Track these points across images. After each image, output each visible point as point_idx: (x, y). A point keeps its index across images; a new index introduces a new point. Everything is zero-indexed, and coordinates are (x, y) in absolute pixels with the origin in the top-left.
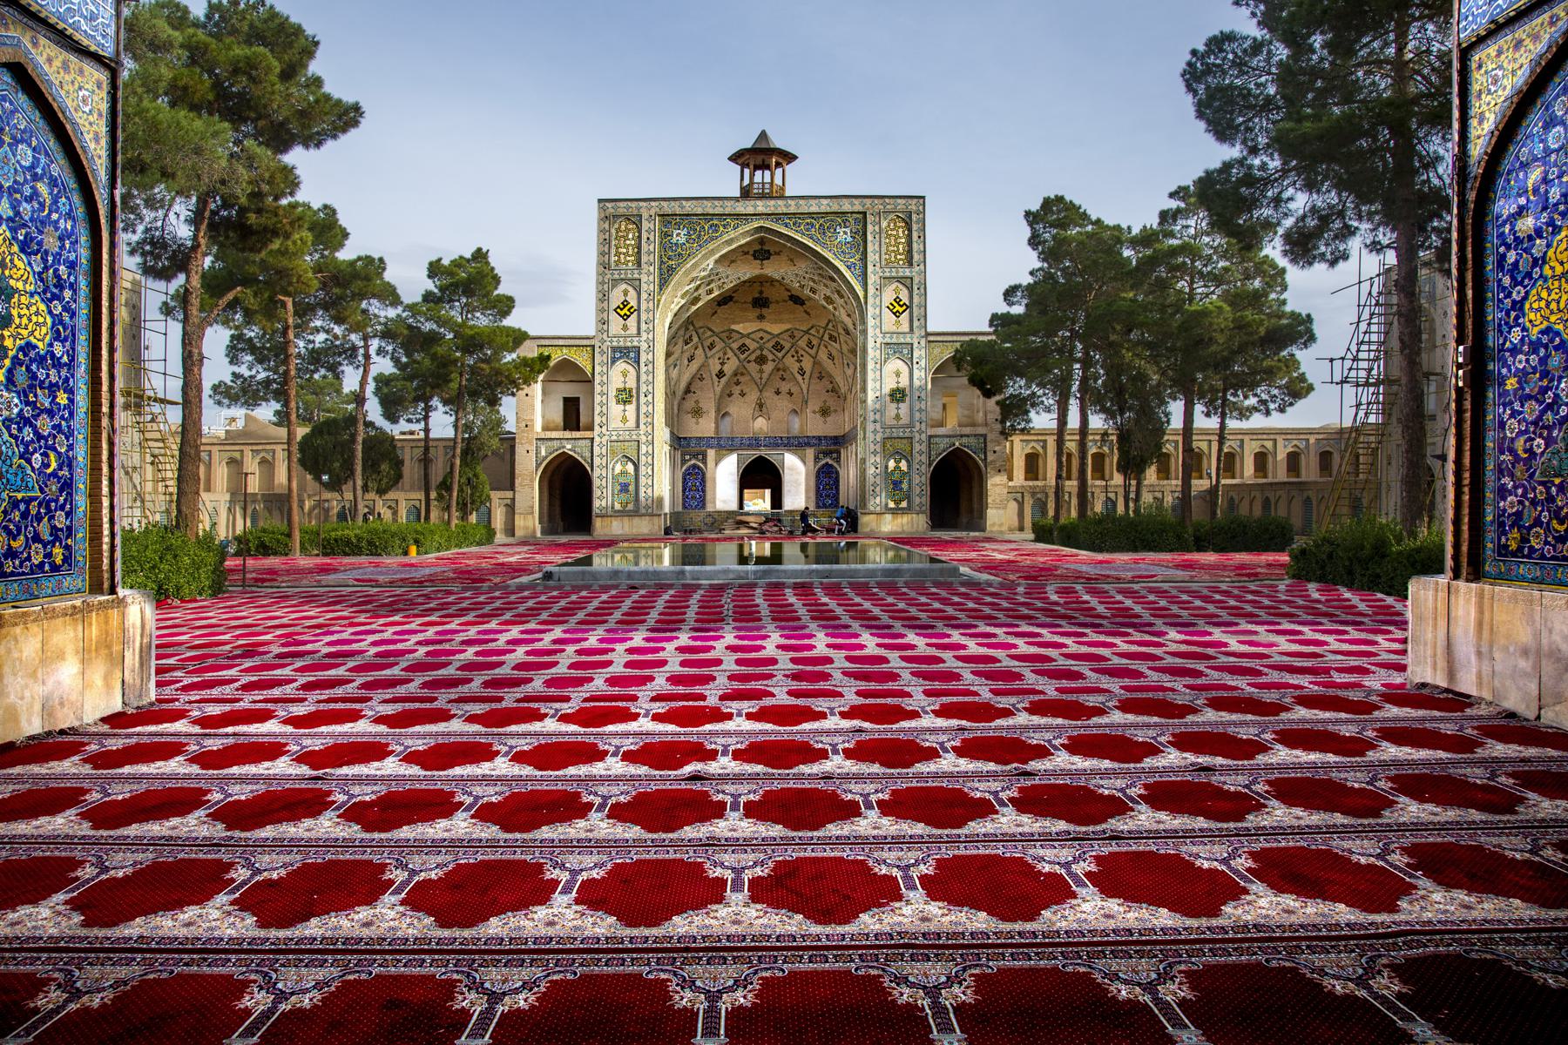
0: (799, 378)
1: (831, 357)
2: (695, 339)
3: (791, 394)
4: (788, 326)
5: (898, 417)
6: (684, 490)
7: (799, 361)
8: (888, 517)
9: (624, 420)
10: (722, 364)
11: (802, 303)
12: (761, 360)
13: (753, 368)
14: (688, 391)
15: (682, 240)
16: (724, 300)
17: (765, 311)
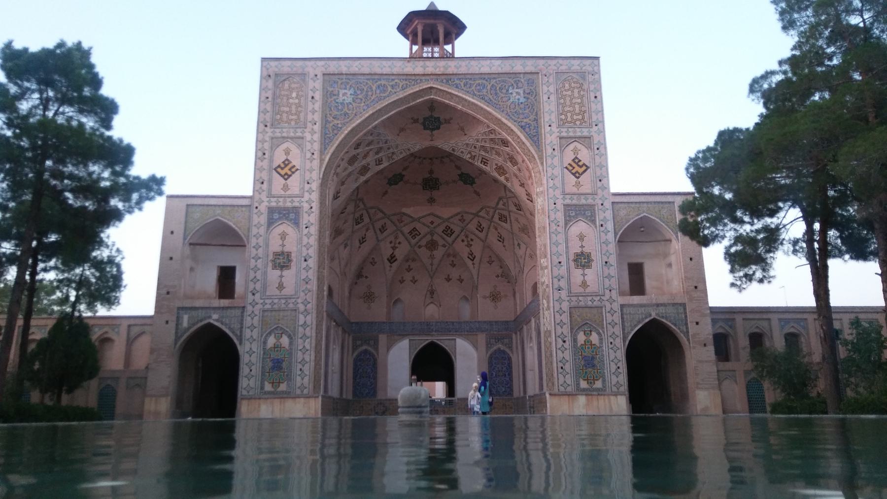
0: (469, 263)
1: (501, 239)
2: (366, 220)
3: (461, 281)
4: (458, 210)
6: (355, 378)
7: (469, 246)
8: (582, 399)
10: (394, 248)
11: (472, 183)
12: (432, 245)
13: (424, 253)
14: (359, 275)
15: (349, 99)
16: (395, 179)
17: (435, 193)
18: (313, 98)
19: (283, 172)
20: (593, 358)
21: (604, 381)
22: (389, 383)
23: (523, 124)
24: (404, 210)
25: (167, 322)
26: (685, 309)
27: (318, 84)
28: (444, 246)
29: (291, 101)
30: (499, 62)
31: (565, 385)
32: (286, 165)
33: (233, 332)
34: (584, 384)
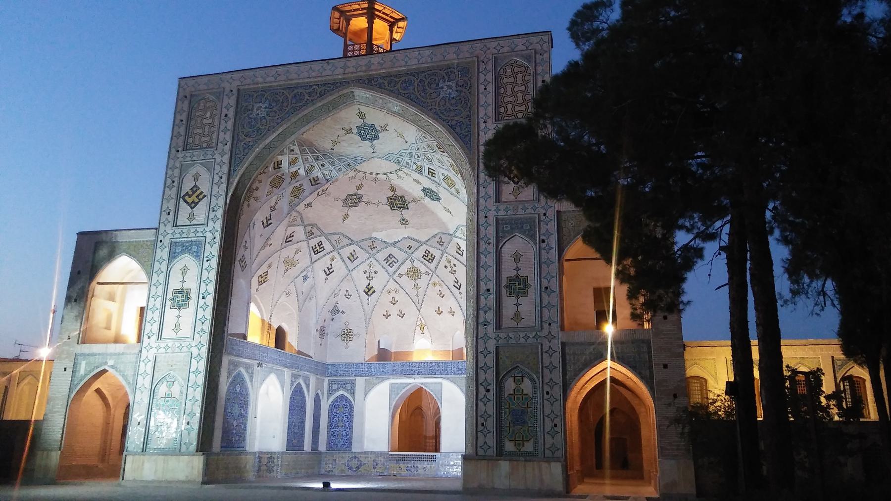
5: (517, 316)
7: (453, 272)
9: (177, 327)
18: (226, 115)
19: (190, 200)
20: (523, 412)
21: (536, 443)
22: (366, 435)
23: (453, 123)
24: (374, 235)
25: (65, 369)
26: (649, 347)
27: (232, 101)
28: (427, 273)
29: (205, 121)
30: (427, 52)
31: (486, 447)
32: (194, 193)
33: (126, 380)
34: (509, 446)
